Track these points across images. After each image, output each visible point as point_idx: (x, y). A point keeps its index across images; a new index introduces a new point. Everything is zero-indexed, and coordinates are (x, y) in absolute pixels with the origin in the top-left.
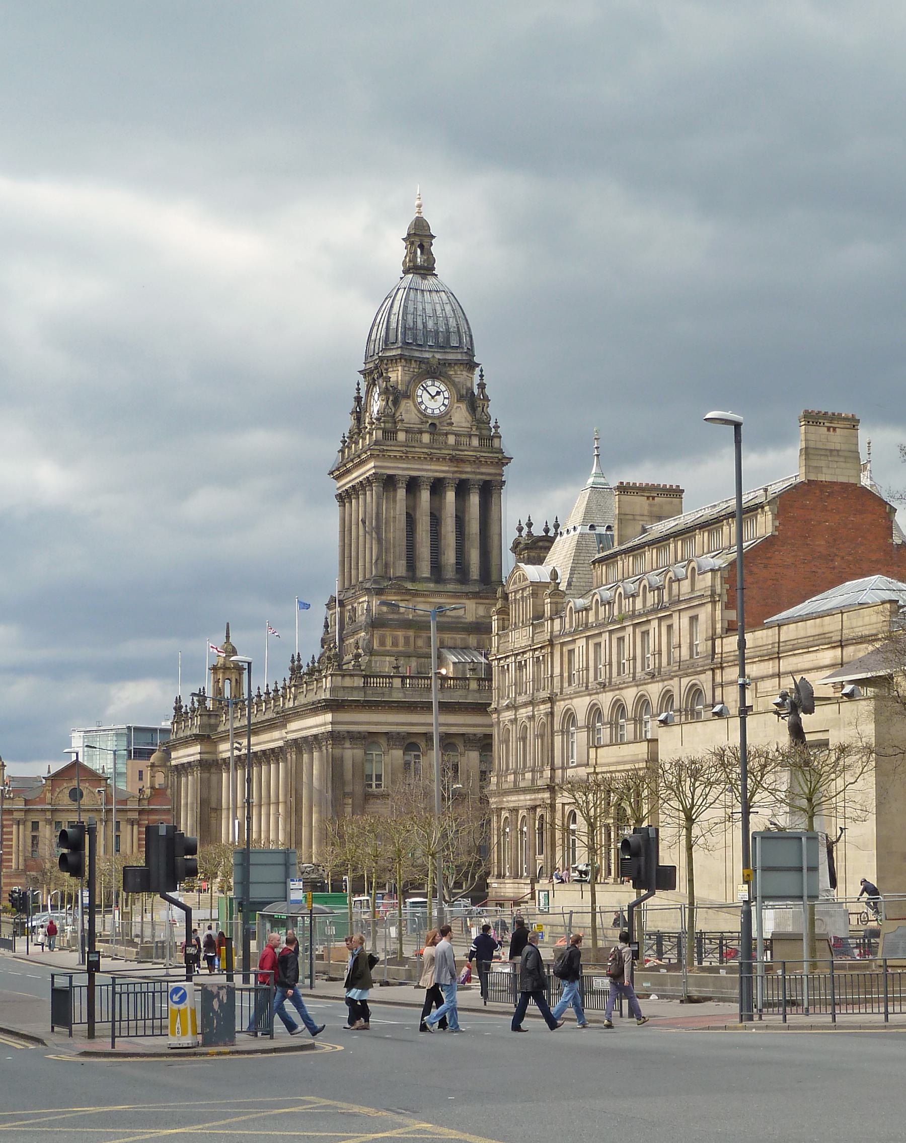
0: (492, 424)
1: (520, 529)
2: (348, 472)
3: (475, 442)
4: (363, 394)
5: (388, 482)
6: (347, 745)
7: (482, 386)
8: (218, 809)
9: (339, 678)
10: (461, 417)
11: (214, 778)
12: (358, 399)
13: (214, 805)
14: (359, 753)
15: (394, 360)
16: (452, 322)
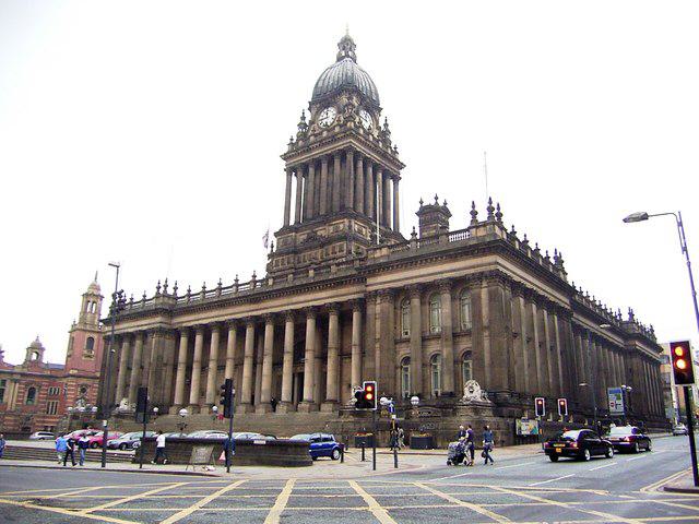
0: (393, 146)
1: (421, 202)
5: (357, 155)
7: (386, 125)
12: (303, 118)
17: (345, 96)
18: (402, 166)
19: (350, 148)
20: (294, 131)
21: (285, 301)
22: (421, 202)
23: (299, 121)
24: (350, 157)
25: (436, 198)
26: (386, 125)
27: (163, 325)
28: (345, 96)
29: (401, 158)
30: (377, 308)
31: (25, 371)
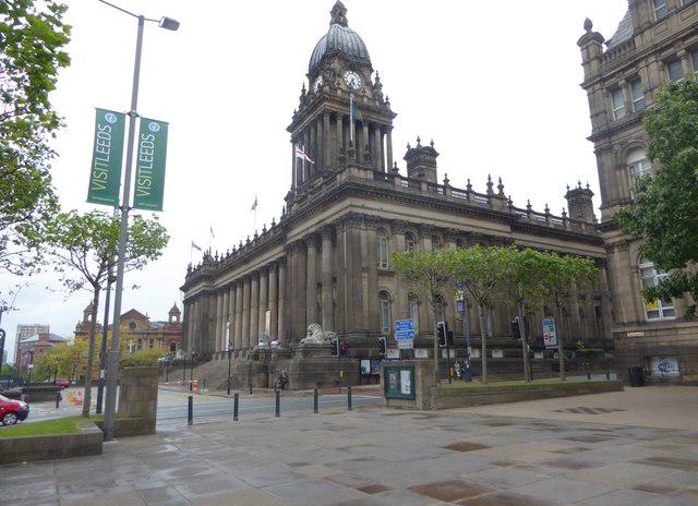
0: (384, 98)
1: (408, 147)
2: (302, 121)
3: (377, 104)
4: (307, 88)
5: (333, 117)
6: (363, 226)
7: (377, 79)
8: (213, 320)
9: (356, 170)
10: (368, 93)
11: (212, 302)
12: (304, 90)
13: (211, 317)
14: (372, 234)
15: (333, 56)
16: (361, 46)
17: (338, 61)
18: (393, 115)
19: (325, 111)
20: (296, 104)
21: (258, 260)
22: (408, 147)
23: (301, 93)
24: (327, 119)
25: (419, 140)
26: (377, 79)
27: (206, 289)
28: (338, 61)
29: (393, 108)
30: (294, 259)
31: (167, 331)
